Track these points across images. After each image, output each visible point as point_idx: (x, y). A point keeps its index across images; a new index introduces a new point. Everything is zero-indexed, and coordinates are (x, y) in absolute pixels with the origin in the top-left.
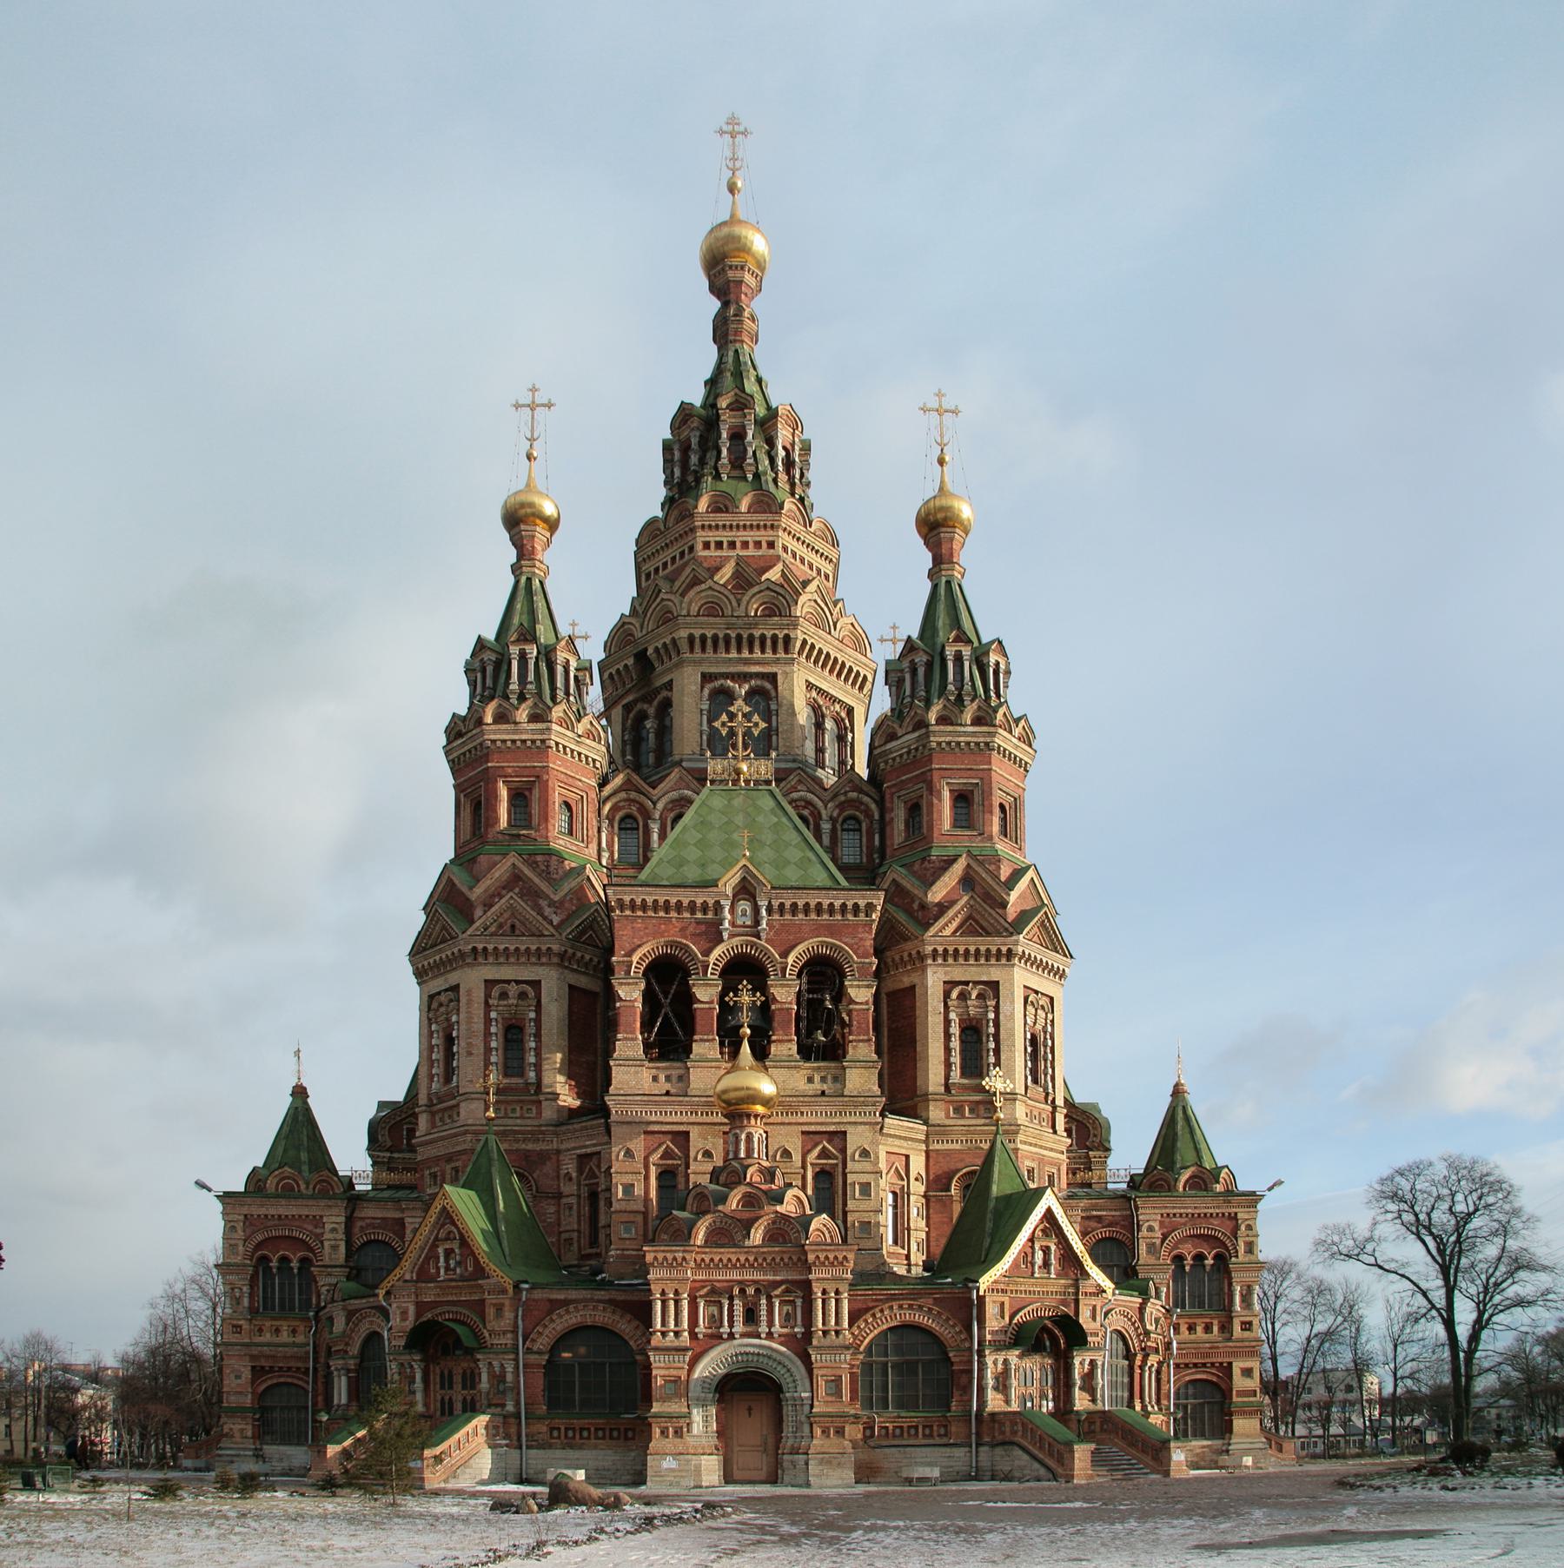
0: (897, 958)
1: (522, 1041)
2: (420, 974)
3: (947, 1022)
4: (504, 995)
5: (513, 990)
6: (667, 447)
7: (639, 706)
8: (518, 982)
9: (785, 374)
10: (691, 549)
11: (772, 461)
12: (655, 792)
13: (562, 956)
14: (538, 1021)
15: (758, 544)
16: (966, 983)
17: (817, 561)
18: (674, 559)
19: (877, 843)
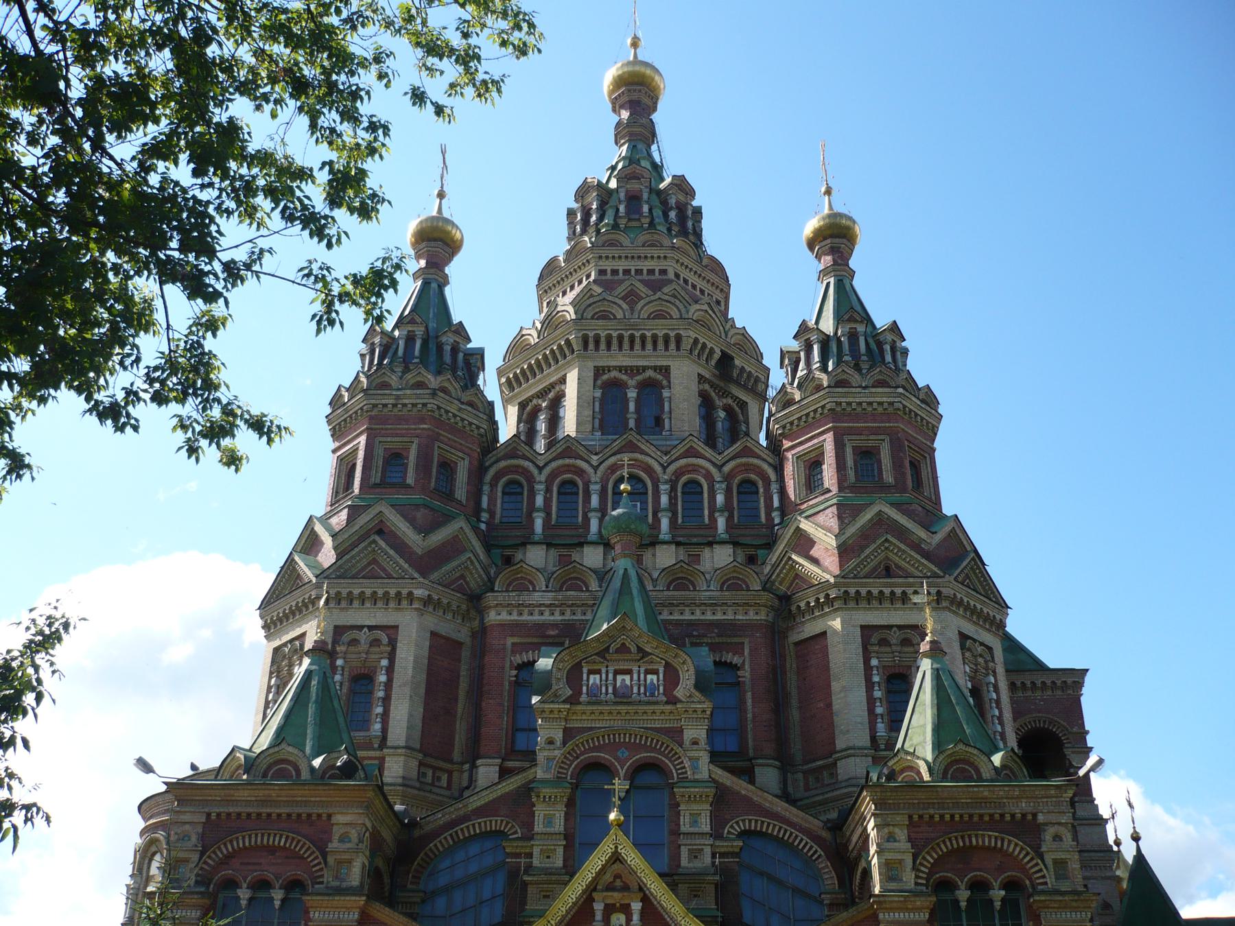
0: (802, 604)
1: (371, 693)
2: (271, 626)
3: (868, 669)
4: (354, 642)
5: (363, 636)
6: (571, 213)
7: (535, 401)
8: (371, 628)
9: (676, 154)
10: (588, 276)
11: (666, 215)
13: (427, 601)
14: (390, 670)
15: (651, 272)
16: (889, 627)
17: (708, 288)
19: (776, 503)
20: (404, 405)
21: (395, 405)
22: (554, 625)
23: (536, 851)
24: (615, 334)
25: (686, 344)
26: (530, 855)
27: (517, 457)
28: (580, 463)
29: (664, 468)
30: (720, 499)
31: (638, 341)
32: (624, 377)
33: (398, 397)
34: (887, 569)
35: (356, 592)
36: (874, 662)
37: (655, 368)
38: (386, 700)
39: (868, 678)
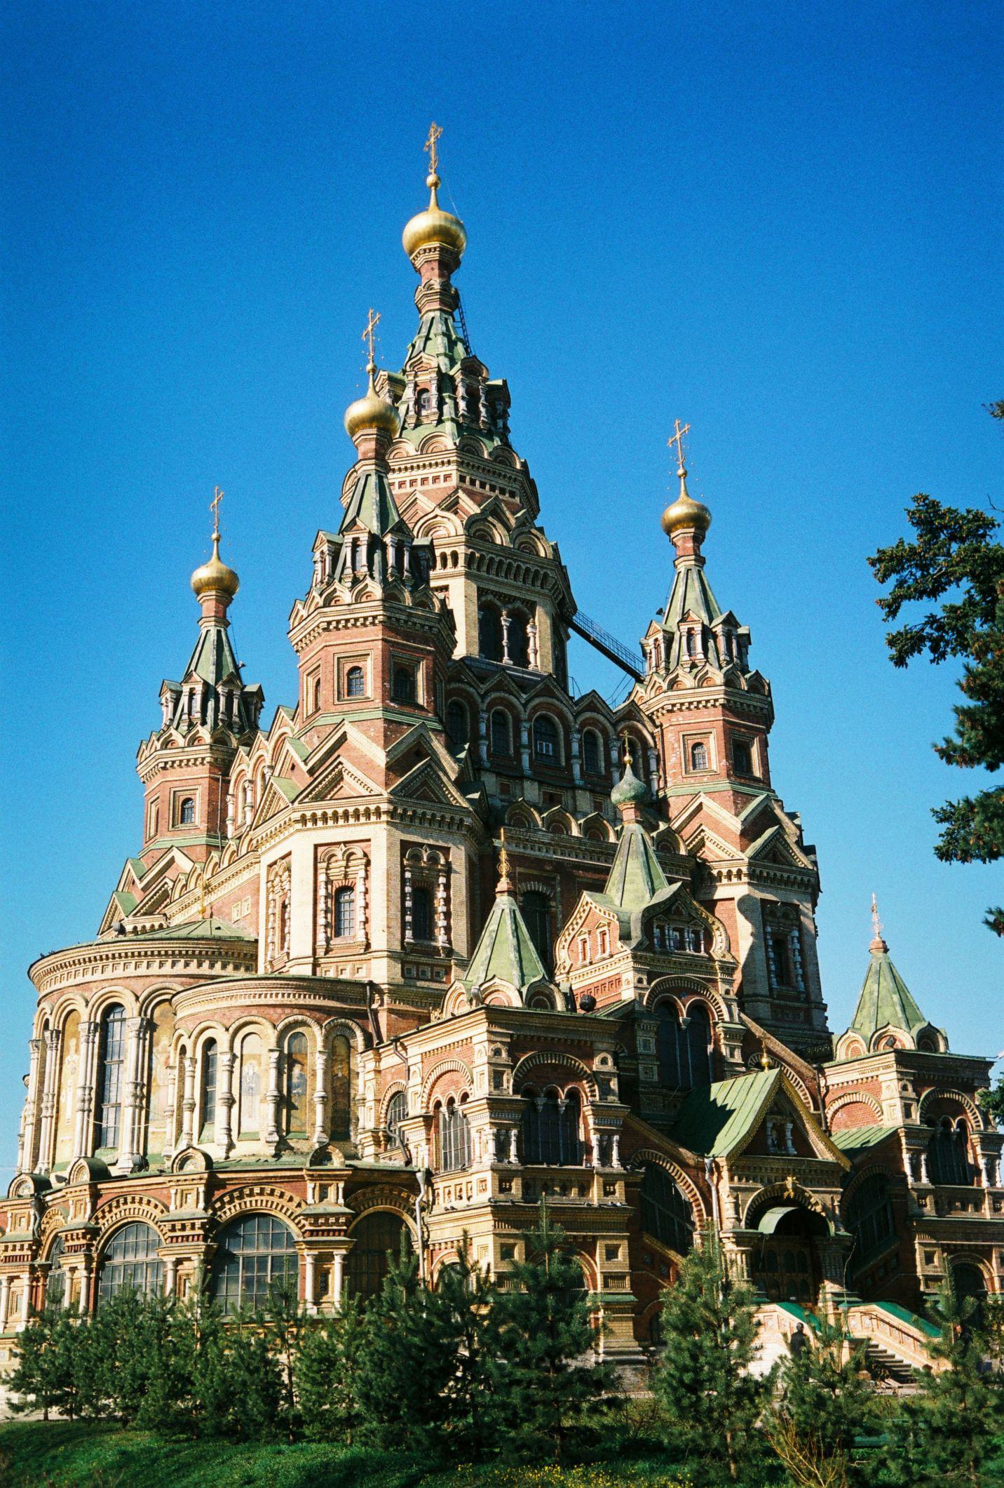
3: (765, 933)
4: (416, 858)
12: (483, 688)
18: (424, 481)
20: (415, 624)
21: (406, 622)
22: (551, 862)
23: (641, 1067)
24: (497, 559)
25: (551, 582)
26: (636, 1070)
27: (462, 681)
28: (514, 700)
29: (575, 717)
30: (614, 754)
31: (513, 571)
32: (499, 603)
33: (410, 615)
34: (774, 855)
35: (420, 811)
36: (769, 929)
37: (524, 601)
38: (448, 915)
39: (766, 940)
